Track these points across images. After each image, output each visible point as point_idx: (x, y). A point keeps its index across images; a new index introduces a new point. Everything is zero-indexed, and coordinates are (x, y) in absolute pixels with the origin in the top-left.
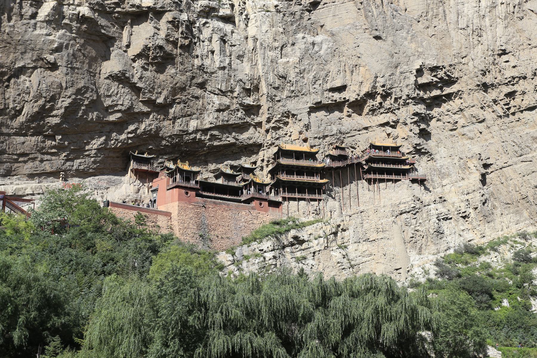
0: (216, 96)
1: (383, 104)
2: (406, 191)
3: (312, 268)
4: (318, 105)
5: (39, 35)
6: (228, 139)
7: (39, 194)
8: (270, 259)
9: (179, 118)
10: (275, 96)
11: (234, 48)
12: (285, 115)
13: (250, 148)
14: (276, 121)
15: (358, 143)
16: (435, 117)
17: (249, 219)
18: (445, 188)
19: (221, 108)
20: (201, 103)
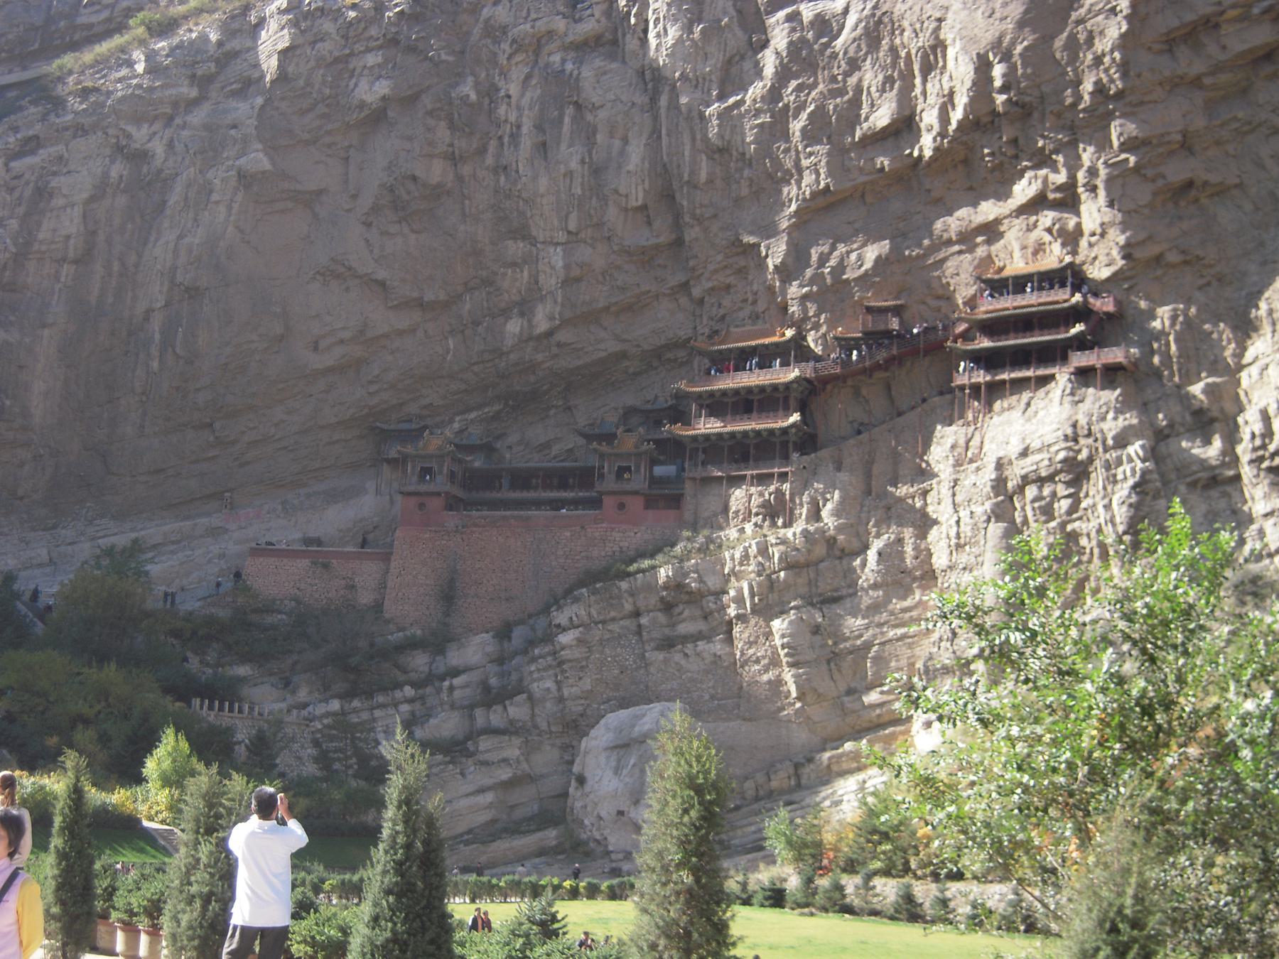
0: (559, 249)
1: (1021, 142)
2: (1055, 408)
4: (821, 201)
5: (167, 243)
6: (602, 346)
7: (173, 543)
8: (563, 649)
9: (479, 324)
10: (702, 206)
11: (602, 114)
13: (670, 355)
14: (716, 271)
16: (1260, 125)
18: (1244, 375)
20: (526, 273)
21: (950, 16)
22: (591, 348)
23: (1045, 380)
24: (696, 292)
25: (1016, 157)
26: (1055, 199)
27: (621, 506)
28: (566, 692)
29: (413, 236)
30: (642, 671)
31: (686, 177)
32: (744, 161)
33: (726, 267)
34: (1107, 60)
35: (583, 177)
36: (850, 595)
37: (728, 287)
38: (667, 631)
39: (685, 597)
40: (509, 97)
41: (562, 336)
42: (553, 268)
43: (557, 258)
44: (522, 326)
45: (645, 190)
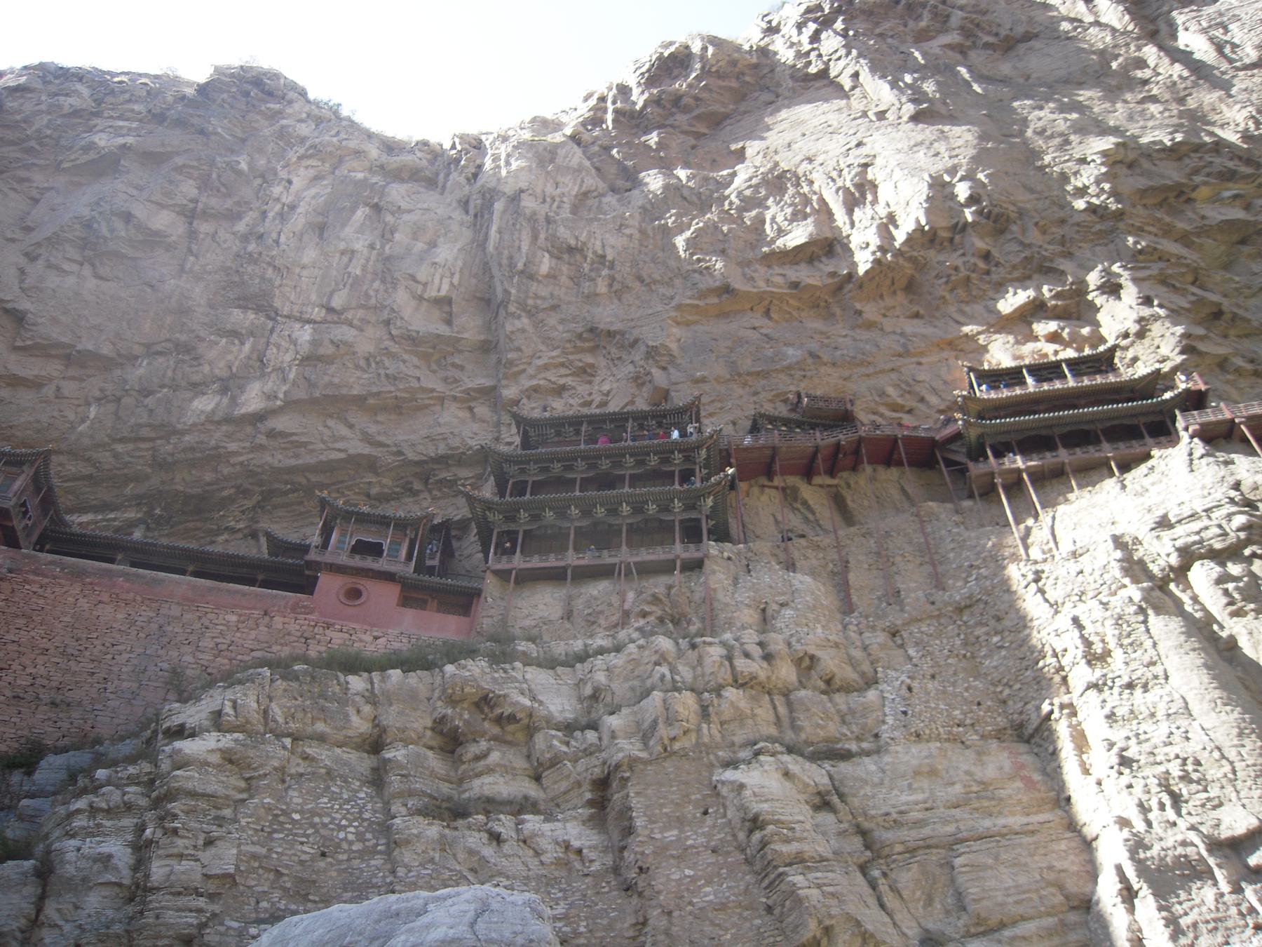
0: (307, 327)
3: (558, 862)
10: (536, 296)
11: (406, 217)
12: (579, 344)
13: (443, 475)
14: (546, 367)
15: (917, 388)
17: (249, 644)
19: (321, 351)
20: (247, 347)
21: (879, 161)
22: (323, 446)
23: (1125, 467)
24: (510, 392)
25: (988, 273)
26: (1056, 306)
27: (354, 594)
28: (158, 870)
29: (92, 283)
30: (377, 861)
31: (520, 266)
32: (603, 264)
33: (563, 365)
34: (1093, 190)
35: (368, 260)
36: (868, 754)
37: (560, 390)
38: (445, 788)
39: (496, 730)
40: (290, 182)
41: (281, 423)
42: (295, 343)
43: (305, 335)
44: (218, 405)
45: (452, 284)
